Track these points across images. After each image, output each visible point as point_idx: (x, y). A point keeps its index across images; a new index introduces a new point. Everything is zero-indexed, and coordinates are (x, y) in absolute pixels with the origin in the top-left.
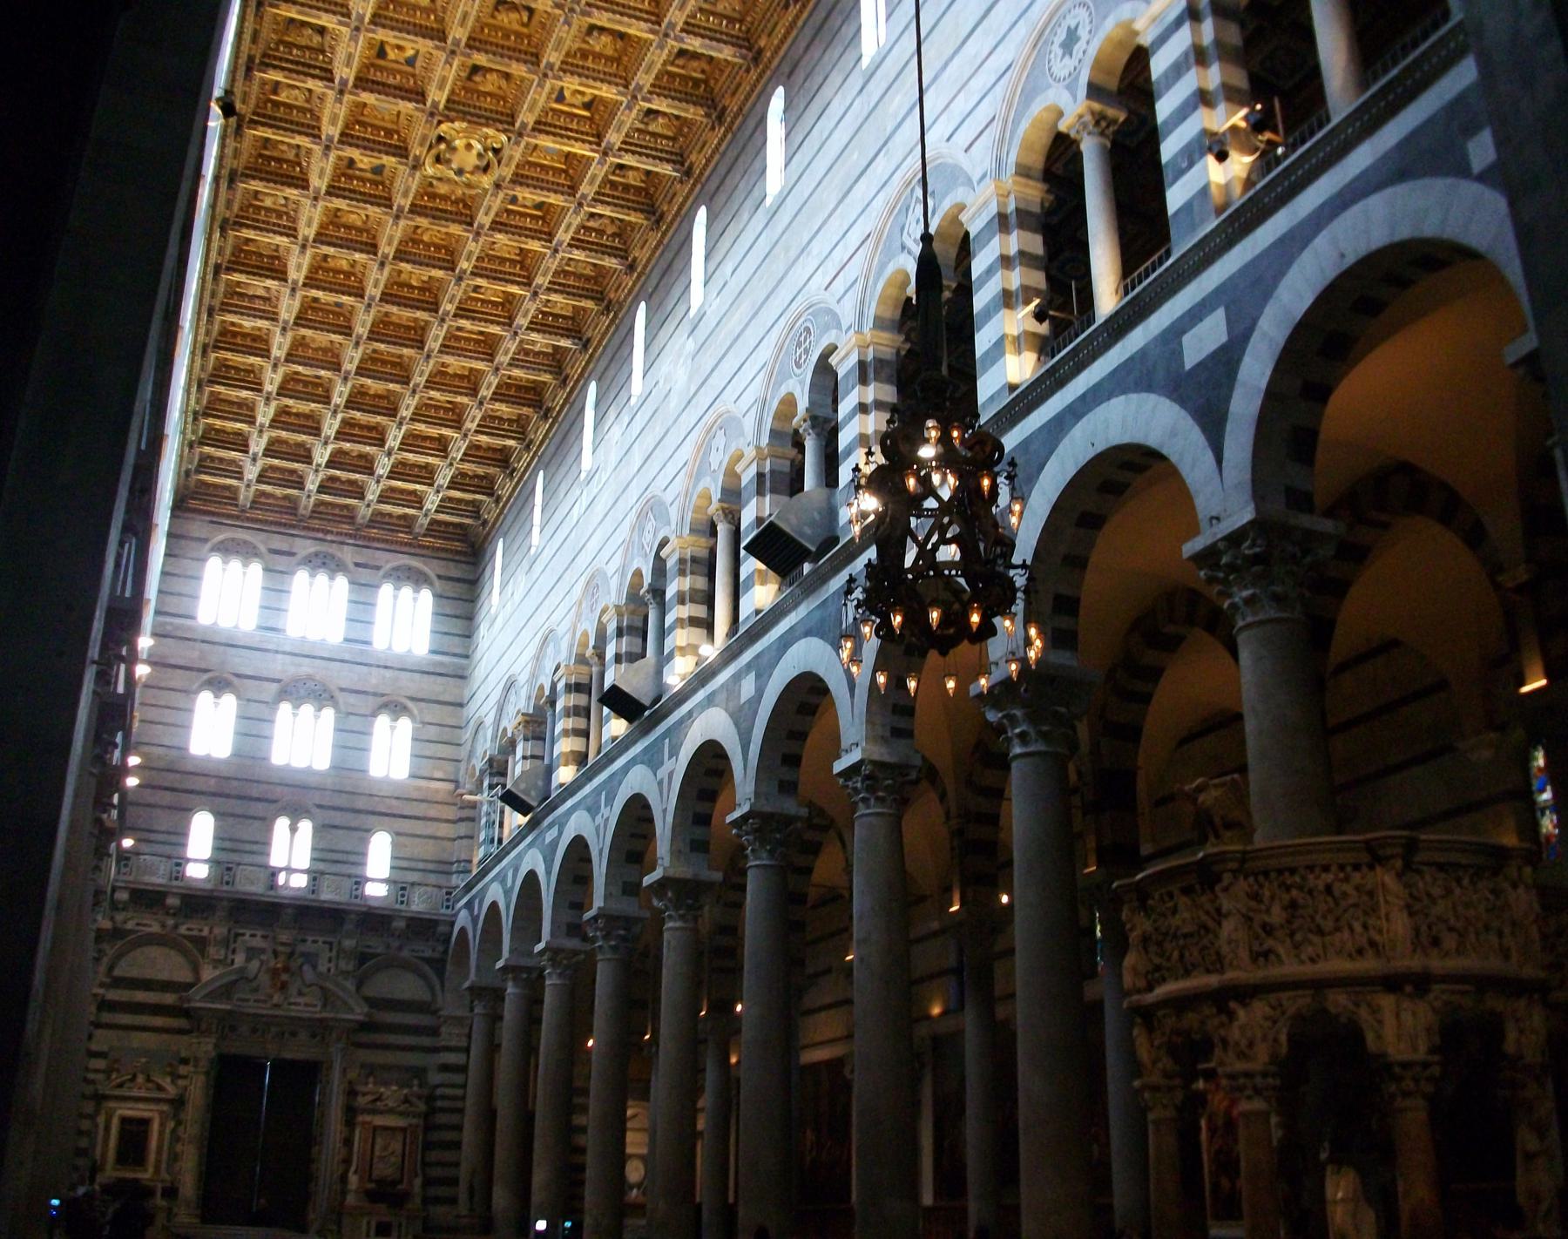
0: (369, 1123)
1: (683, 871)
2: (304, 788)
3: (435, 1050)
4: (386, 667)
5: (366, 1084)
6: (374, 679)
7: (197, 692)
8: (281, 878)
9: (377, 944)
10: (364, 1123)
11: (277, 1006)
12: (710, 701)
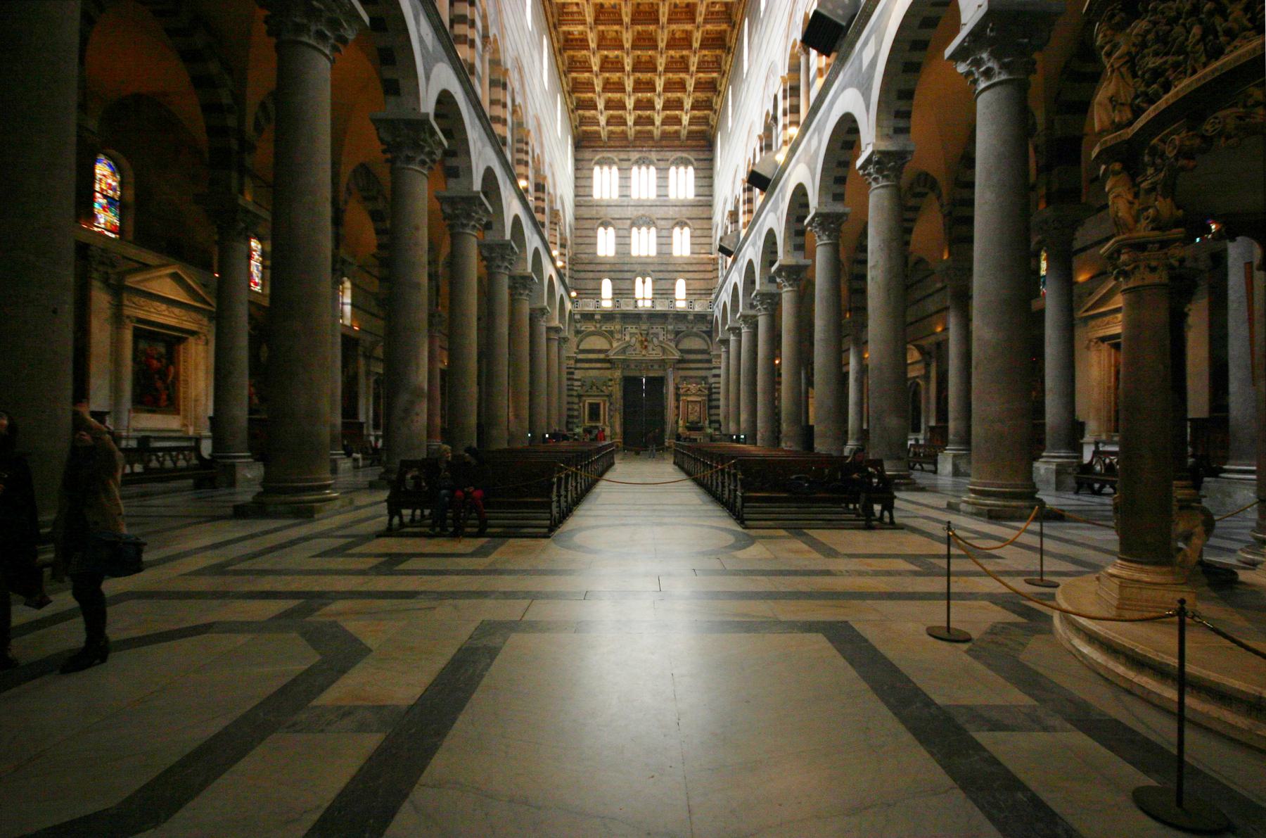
1: (791, 261)
3: (710, 369)
4: (676, 206)
6: (671, 212)
7: (597, 229)
8: (640, 304)
9: (683, 327)
11: (644, 356)
12: (798, 162)
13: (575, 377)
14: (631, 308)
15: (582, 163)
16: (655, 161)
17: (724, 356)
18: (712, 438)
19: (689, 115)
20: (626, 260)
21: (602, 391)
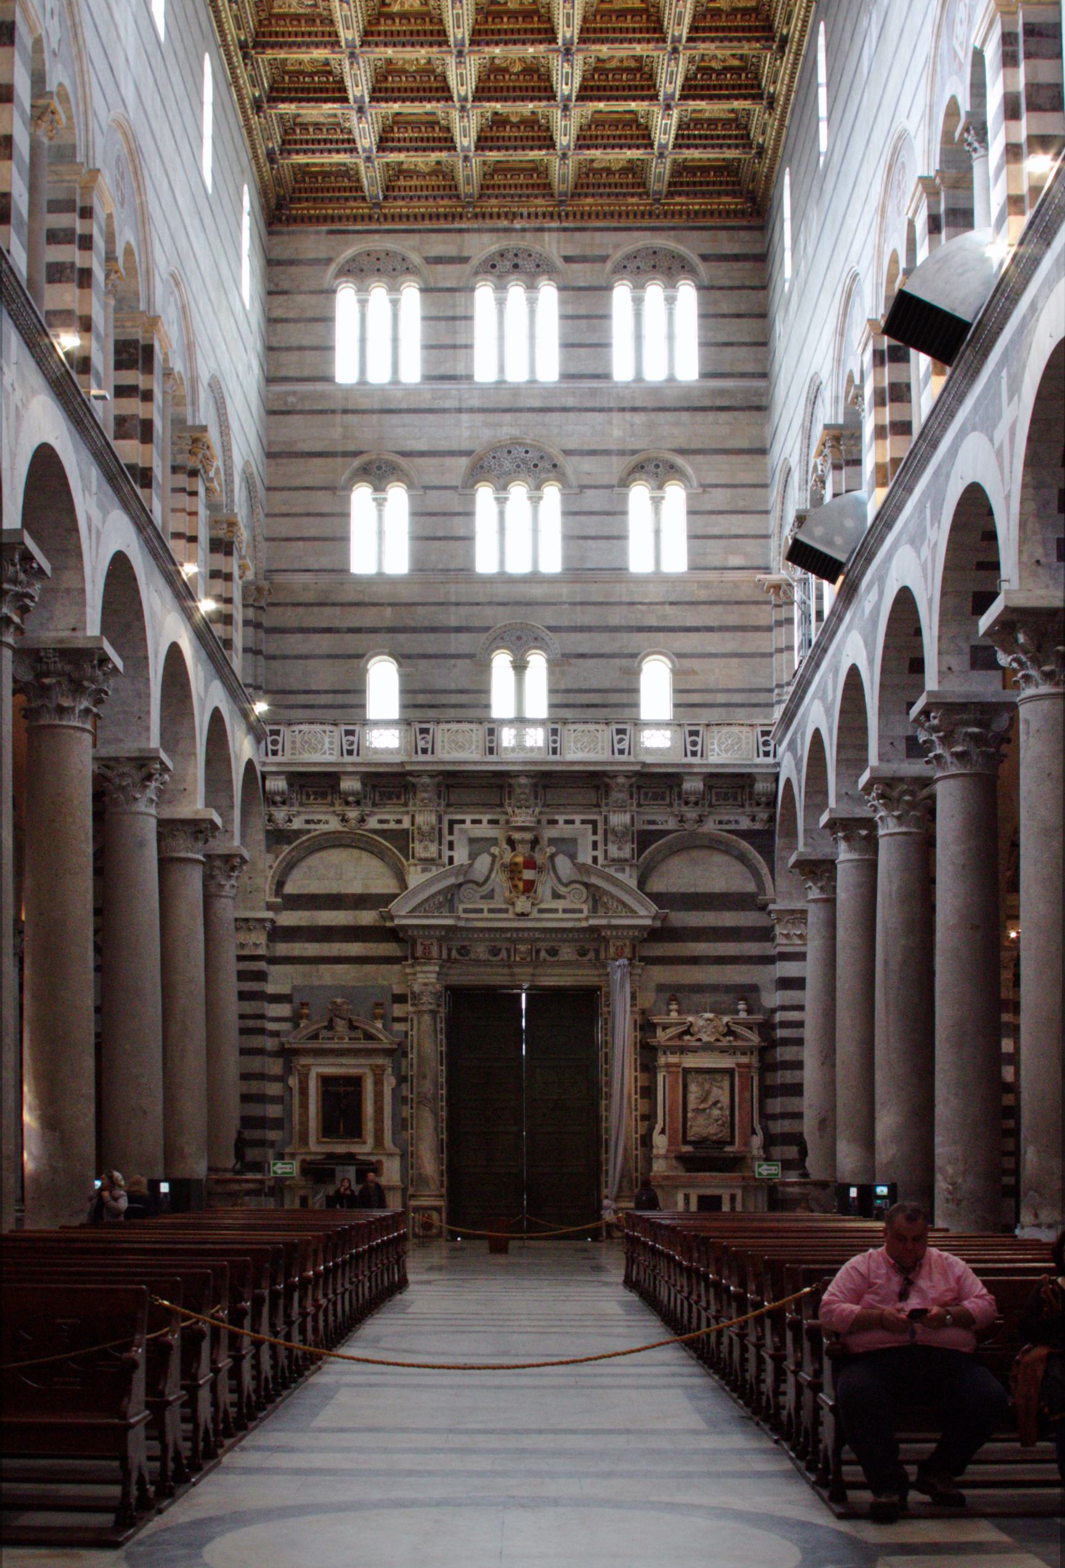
0: (677, 1065)
2: (528, 604)
5: (669, 1011)
8: (507, 737)
10: (668, 1065)
11: (523, 915)
13: (271, 988)
14: (476, 756)
15: (293, 269)
16: (559, 263)
17: (815, 914)
18: (776, 1199)
19: (675, 113)
20: (454, 591)
21: (369, 1037)
